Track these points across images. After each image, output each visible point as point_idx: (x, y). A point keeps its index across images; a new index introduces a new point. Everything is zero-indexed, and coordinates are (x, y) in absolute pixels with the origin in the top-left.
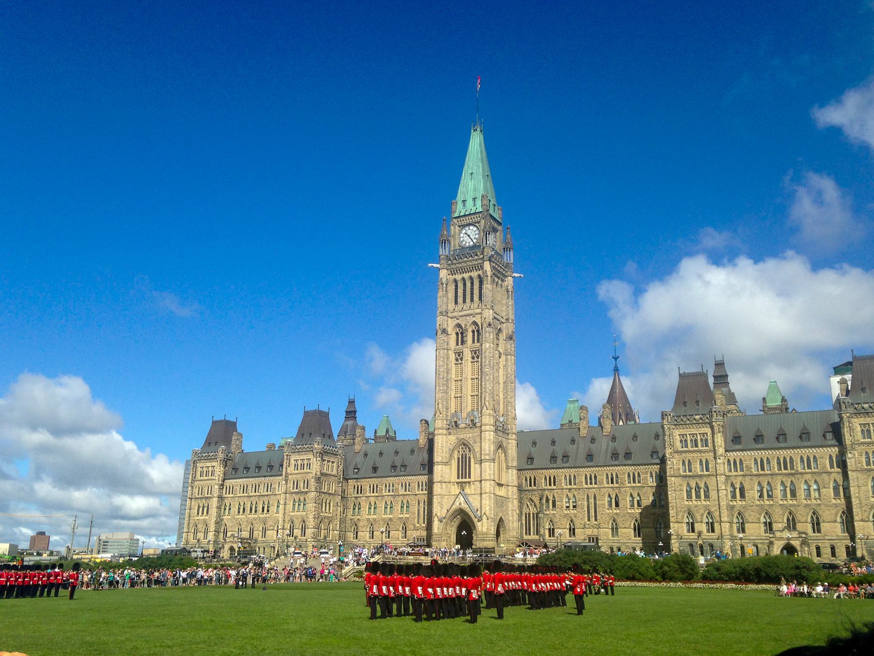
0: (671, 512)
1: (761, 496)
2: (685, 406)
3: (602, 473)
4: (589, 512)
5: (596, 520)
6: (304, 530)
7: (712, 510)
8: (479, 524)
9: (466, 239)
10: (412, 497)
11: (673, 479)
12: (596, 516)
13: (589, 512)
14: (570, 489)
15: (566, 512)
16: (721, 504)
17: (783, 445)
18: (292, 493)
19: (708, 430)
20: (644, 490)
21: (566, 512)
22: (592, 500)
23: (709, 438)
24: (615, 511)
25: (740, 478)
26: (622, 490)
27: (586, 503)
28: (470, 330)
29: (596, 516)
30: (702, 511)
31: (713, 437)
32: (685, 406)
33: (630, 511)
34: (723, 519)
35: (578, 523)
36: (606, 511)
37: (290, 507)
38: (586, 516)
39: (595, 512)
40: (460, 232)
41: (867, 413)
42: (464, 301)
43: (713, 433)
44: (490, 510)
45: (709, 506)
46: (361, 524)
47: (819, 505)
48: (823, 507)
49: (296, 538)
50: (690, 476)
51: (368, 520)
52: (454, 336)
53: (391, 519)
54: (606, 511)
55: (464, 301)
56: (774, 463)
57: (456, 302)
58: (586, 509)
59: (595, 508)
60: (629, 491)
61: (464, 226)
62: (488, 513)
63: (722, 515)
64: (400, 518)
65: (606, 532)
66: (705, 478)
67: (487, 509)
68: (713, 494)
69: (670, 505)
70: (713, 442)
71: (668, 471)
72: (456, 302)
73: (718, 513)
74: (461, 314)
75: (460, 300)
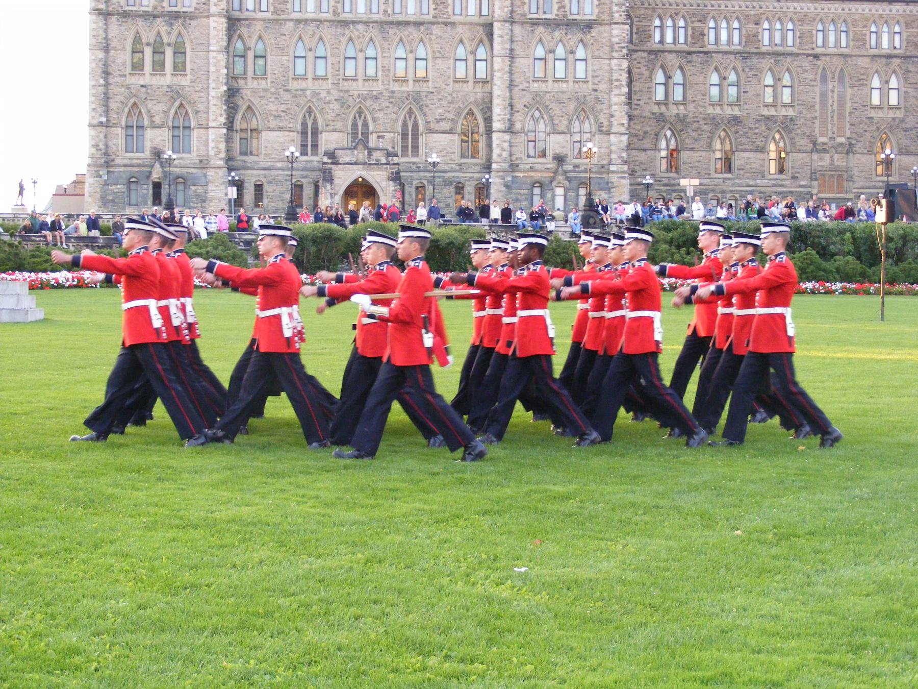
18: (535, 23)
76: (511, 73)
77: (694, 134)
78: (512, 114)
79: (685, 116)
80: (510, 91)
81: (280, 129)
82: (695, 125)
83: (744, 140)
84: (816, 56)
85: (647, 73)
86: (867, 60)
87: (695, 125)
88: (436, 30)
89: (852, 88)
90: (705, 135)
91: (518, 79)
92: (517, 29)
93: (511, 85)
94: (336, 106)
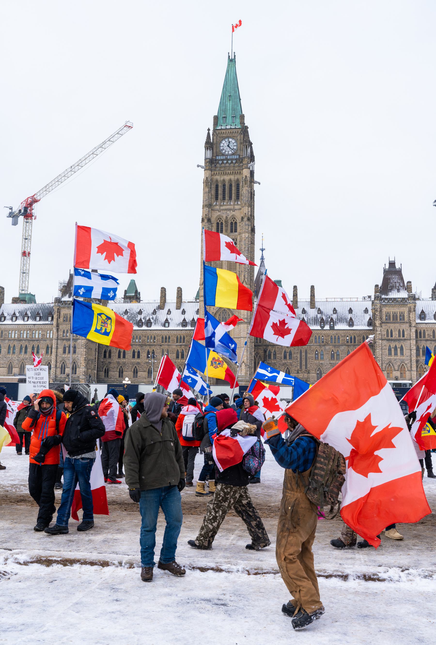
6: (74, 369)
9: (226, 148)
10: (158, 347)
11: (380, 341)
15: (284, 361)
16: (412, 359)
18: (63, 340)
21: (284, 361)
22: (303, 354)
27: (299, 356)
28: (230, 222)
30: (399, 363)
34: (413, 369)
37: (61, 350)
38: (299, 364)
40: (221, 142)
42: (224, 198)
44: (247, 360)
45: (403, 360)
46: (112, 366)
49: (68, 375)
50: (392, 340)
51: (118, 363)
52: (215, 225)
53: (138, 363)
55: (224, 198)
57: (217, 198)
58: (299, 360)
61: (224, 138)
62: (245, 361)
63: (413, 366)
64: (147, 363)
65: (314, 376)
67: (245, 358)
68: (406, 352)
72: (217, 198)
73: (409, 365)
74: (221, 208)
75: (220, 197)
76: (57, 352)
77: (127, 367)
78: (56, 363)
79: (125, 362)
80: (56, 358)
81: (3, 367)
82: (128, 365)
83: (141, 369)
84: (161, 346)
85: (115, 351)
86: (175, 346)
87: (128, 365)
88: (41, 342)
89: (171, 354)
90: (130, 367)
91: (59, 354)
92: (59, 341)
93: (57, 355)
94: (17, 361)
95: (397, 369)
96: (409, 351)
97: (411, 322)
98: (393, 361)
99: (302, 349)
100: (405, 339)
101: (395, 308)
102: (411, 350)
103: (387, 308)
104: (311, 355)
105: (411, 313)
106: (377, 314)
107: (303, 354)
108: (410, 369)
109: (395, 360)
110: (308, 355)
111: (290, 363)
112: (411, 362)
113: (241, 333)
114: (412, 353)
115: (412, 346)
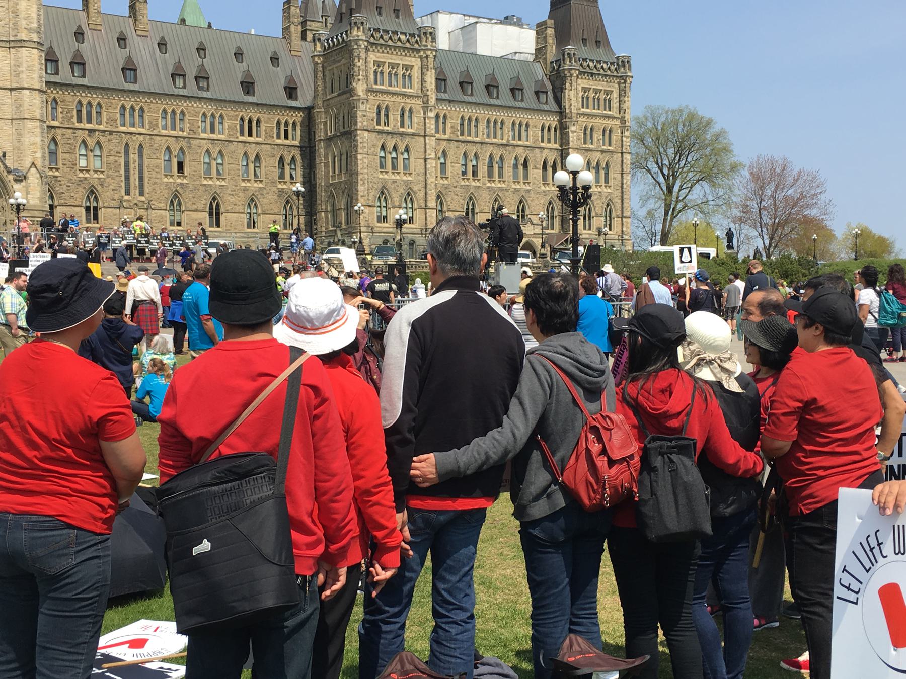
0: (361, 188)
1: (464, 173)
2: (380, 14)
3: (154, 110)
4: (127, 178)
5: (141, 193)
7: (415, 189)
8: (16, 186)
11: (366, 134)
12: (141, 186)
13: (127, 178)
14: (91, 131)
16: (429, 182)
17: (470, 99)
19: (416, 62)
20: (232, 147)
22: (134, 157)
23: (416, 73)
24: (179, 181)
25: (445, 143)
26: (193, 142)
27: (122, 161)
29: (141, 186)
31: (422, 74)
32: (380, 14)
33: (205, 182)
34: (429, 204)
35: (106, 197)
36: (161, 182)
38: (123, 184)
39: (141, 179)
41: (592, 75)
43: (424, 69)
45: (411, 182)
47: (528, 191)
48: (532, 195)
50: (388, 133)
54: (161, 182)
56: (482, 126)
58: (122, 172)
59: (141, 172)
60: (206, 145)
62: (39, 163)
63: (429, 198)
65: (162, 217)
66: (408, 139)
68: (416, 164)
69: (360, 177)
70: (423, 81)
71: (359, 119)
73: (422, 194)
95: (397, 204)
96: (423, 161)
97: (429, 93)
98: (389, 184)
99: (130, 144)
100: (414, 135)
101: (394, 57)
102: (425, 160)
103: (378, 54)
104: (154, 162)
105: (429, 73)
106: (359, 64)
107: (134, 157)
108: (423, 206)
109: (394, 182)
110: (146, 162)
111: (99, 179)
112: (426, 187)
113: (23, 76)
114: (428, 166)
115: (428, 152)
